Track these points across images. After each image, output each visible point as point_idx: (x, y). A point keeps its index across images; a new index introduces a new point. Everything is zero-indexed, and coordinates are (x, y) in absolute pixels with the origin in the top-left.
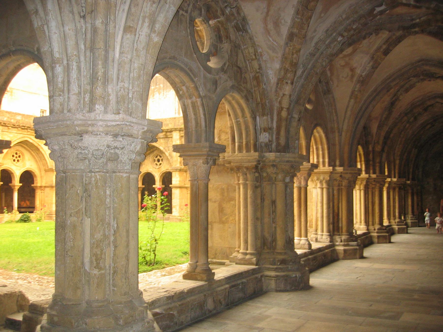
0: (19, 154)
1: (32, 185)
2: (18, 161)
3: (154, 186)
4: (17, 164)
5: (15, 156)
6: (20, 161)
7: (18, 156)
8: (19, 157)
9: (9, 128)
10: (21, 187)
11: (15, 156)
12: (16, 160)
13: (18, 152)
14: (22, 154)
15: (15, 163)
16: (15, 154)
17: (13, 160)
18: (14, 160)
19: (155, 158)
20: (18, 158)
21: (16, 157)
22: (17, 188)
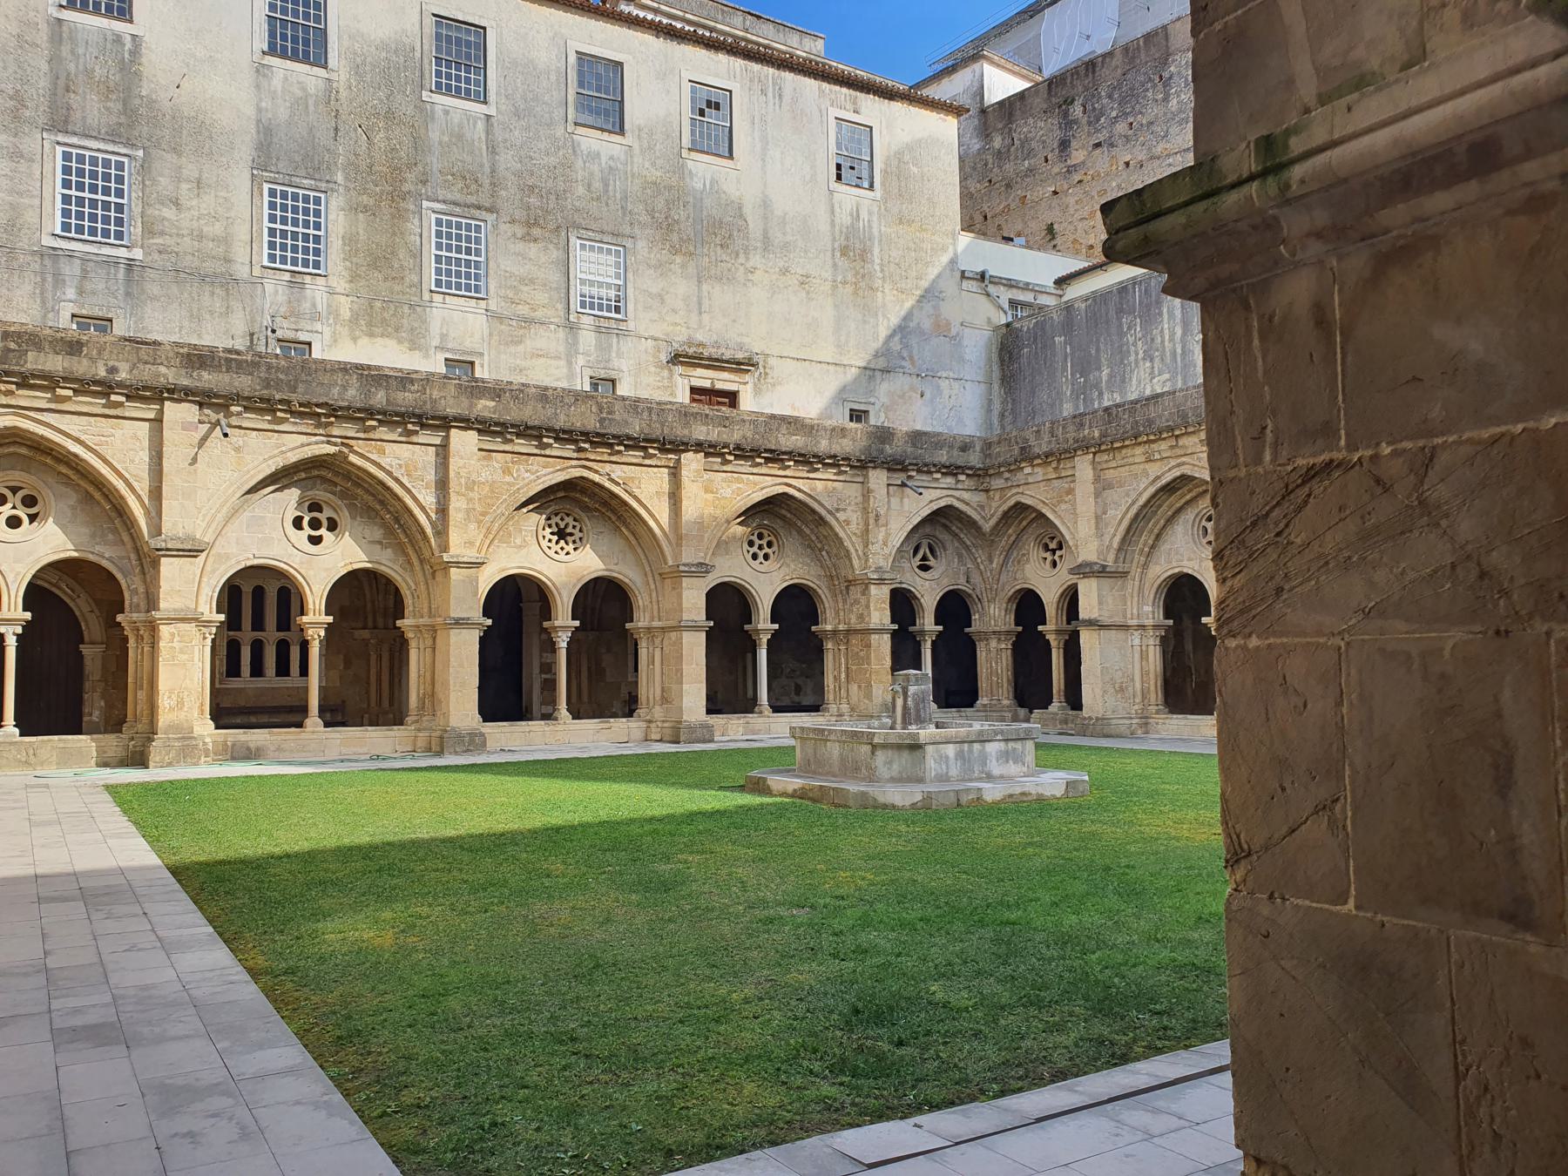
1: (814, 628)
2: (766, 557)
3: (1040, 628)
4: (761, 568)
5: (757, 542)
7: (764, 542)
8: (770, 545)
10: (775, 634)
11: (757, 542)
12: (761, 554)
13: (765, 532)
14: (775, 536)
15: (755, 564)
16: (755, 538)
17: (749, 557)
18: (755, 557)
19: (1204, 523)
20: (767, 550)
21: (760, 547)
22: (765, 638)
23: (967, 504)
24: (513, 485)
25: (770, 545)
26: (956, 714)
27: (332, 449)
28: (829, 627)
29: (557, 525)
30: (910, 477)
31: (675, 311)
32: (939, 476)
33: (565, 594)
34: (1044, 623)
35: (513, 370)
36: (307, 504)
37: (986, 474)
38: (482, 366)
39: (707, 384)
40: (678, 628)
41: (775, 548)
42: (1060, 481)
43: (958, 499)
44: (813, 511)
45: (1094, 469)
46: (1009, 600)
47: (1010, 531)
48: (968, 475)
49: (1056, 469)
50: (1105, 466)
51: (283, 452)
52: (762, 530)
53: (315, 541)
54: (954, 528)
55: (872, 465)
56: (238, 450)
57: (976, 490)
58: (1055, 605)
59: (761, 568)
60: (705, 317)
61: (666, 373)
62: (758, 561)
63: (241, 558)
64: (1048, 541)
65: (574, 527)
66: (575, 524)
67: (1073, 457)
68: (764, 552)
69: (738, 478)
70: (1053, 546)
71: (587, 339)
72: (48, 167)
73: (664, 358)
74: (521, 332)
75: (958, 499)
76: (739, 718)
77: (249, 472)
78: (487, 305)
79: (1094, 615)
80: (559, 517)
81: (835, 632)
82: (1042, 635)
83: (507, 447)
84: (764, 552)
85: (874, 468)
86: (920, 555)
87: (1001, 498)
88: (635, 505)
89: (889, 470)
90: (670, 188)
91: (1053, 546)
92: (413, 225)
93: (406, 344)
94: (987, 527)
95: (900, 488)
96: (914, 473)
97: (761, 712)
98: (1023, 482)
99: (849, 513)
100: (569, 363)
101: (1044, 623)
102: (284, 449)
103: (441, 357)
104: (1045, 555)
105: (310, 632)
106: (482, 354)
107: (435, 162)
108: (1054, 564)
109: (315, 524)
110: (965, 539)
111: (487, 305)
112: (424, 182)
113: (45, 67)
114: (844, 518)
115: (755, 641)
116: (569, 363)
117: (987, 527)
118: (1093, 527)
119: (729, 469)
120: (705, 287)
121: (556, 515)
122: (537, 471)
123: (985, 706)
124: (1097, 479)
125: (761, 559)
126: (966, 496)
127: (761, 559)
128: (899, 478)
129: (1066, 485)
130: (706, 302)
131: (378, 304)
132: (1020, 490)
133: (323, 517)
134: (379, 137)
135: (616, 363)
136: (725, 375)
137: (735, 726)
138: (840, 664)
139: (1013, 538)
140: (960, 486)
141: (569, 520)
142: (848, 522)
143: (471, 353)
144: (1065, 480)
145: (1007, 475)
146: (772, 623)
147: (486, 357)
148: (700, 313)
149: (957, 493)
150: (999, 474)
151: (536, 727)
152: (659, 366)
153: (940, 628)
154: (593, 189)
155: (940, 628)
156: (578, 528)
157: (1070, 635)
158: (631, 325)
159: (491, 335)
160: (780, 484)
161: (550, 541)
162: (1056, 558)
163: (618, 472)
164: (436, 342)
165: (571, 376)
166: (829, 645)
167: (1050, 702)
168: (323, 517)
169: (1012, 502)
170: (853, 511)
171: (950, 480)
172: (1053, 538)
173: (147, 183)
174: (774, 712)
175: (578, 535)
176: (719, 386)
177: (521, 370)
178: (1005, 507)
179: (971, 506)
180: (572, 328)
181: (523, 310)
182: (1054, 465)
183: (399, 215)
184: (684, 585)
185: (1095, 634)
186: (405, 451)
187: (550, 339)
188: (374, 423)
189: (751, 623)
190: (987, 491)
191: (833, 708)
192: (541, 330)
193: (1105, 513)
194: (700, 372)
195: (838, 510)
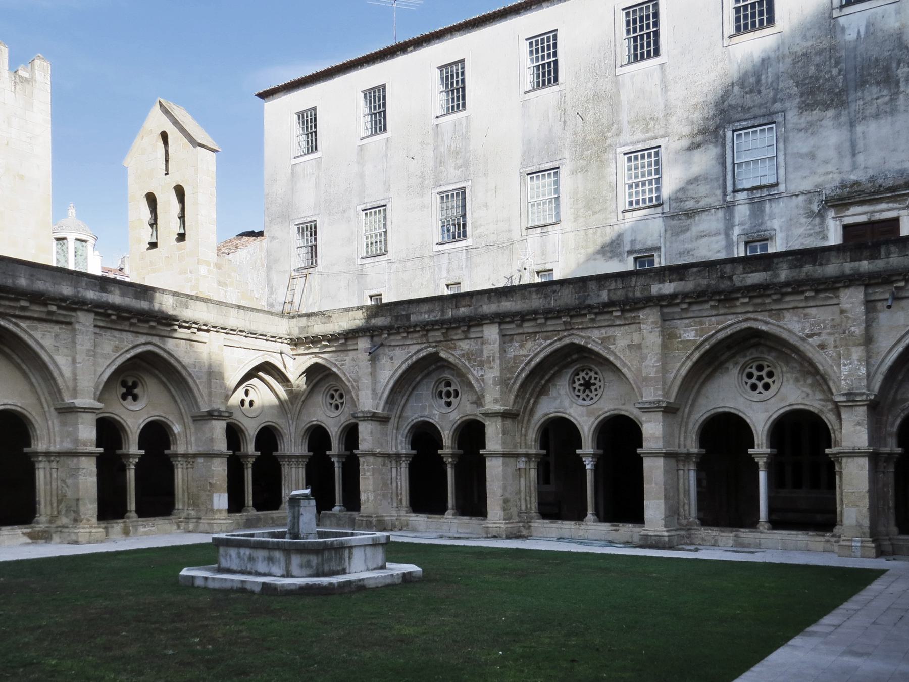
0: (768, 366)
2: (767, 387)
4: (761, 397)
5: (756, 374)
13: (765, 364)
17: (748, 387)
20: (766, 380)
21: (760, 378)
24: (527, 356)
25: (770, 375)
27: (431, 350)
29: (584, 378)
31: (826, 162)
33: (586, 429)
35: (681, 254)
36: (444, 383)
38: (660, 256)
39: (863, 219)
40: (505, 455)
51: (411, 356)
52: (760, 362)
53: (449, 404)
56: (391, 358)
59: (761, 397)
60: (860, 158)
61: (817, 220)
63: (413, 418)
65: (596, 379)
66: (596, 376)
69: (701, 321)
71: (742, 211)
72: (434, 208)
73: (815, 208)
74: (689, 222)
77: (397, 370)
78: (663, 209)
80: (585, 372)
83: (521, 331)
88: (612, 358)
90: (820, 53)
92: (611, 169)
93: (609, 254)
99: (824, 337)
100: (727, 235)
102: (410, 354)
103: (631, 259)
105: (445, 460)
106: (658, 249)
107: (625, 117)
109: (449, 394)
111: (663, 209)
112: (618, 135)
113: (432, 154)
114: (818, 342)
116: (727, 235)
120: (859, 129)
121: (583, 371)
122: (542, 344)
125: (760, 388)
127: (760, 388)
130: (860, 144)
131: (591, 231)
133: (451, 389)
134: (589, 118)
135: (768, 224)
136: (884, 206)
137: (724, 539)
141: (592, 374)
142: (822, 346)
143: (647, 250)
147: (663, 249)
148: (854, 155)
151: (567, 527)
152: (811, 215)
154: (746, 84)
156: (598, 380)
158: (782, 188)
159: (665, 231)
161: (579, 391)
163: (596, 334)
164: (627, 248)
165: (729, 245)
168: (445, 390)
170: (829, 334)
173: (473, 199)
175: (598, 384)
176: (877, 217)
177: (688, 252)
180: (729, 207)
181: (690, 204)
183: (603, 164)
186: (465, 345)
187: (712, 222)
188: (444, 331)
192: (704, 216)
194: (854, 210)
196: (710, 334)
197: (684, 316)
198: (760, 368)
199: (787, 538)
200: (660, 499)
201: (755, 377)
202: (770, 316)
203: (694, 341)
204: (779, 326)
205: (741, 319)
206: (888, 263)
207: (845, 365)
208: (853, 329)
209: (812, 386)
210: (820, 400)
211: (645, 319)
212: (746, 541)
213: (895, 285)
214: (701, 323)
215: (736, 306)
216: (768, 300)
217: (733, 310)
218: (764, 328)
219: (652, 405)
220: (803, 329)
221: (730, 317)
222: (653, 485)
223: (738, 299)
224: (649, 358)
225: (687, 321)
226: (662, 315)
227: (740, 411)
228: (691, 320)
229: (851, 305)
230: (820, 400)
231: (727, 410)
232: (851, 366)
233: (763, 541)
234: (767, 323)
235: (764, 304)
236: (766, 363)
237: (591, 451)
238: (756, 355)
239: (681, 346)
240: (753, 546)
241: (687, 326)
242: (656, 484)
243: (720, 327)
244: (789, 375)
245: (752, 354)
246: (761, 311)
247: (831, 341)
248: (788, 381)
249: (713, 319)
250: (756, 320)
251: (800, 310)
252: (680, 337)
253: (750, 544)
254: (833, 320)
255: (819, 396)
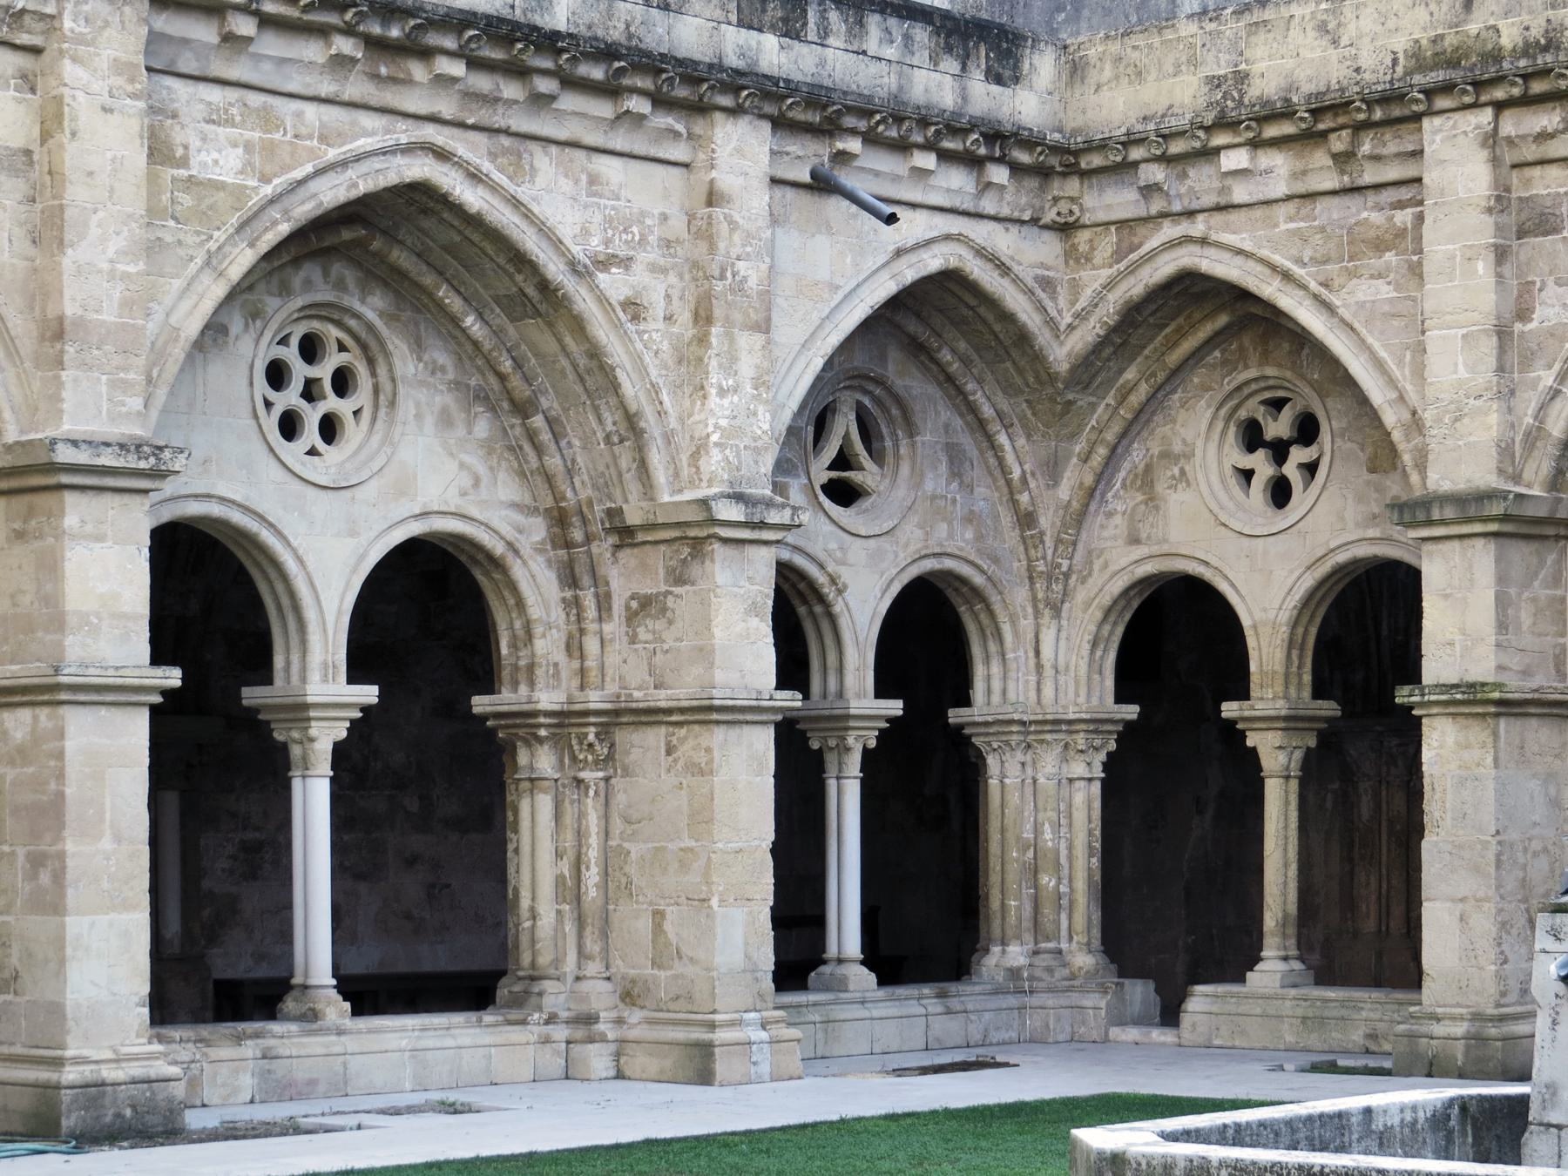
0: (342, 348)
1: (481, 704)
4: (315, 470)
5: (300, 371)
6: (353, 433)
7: (323, 372)
9: (228, 38)
10: (365, 725)
11: (300, 371)
14: (364, 347)
15: (292, 452)
16: (291, 354)
17: (271, 423)
18: (289, 426)
20: (331, 403)
21: (310, 392)
22: (326, 735)
23: (1004, 269)
25: (342, 382)
26: (935, 1006)
28: (548, 699)
30: (842, 157)
32: (927, 160)
34: (1243, 694)
37: (1072, 170)
41: (361, 396)
42: (1353, 202)
43: (980, 252)
44: (521, 260)
45: (1495, 161)
46: (1108, 612)
47: (1130, 374)
48: (1016, 169)
49: (1343, 160)
50: (1530, 152)
52: (316, 325)
54: (946, 356)
55: (726, 101)
57: (1034, 221)
58: (1284, 631)
62: (301, 445)
64: (1260, 414)
67: (1417, 118)
68: (322, 408)
69: (266, 108)
70: (1278, 427)
75: (980, 252)
76: (239, 1039)
79: (1482, 668)
81: (566, 719)
82: (1232, 734)
84: (322, 408)
85: (735, 112)
86: (830, 452)
87: (1118, 256)
89: (781, 124)
91: (1278, 427)
94: (1061, 353)
95: (805, 199)
96: (854, 145)
97: (311, 1016)
98: (1209, 200)
101: (1243, 694)
104: (1248, 461)
108: (1280, 493)
110: (979, 397)
115: (284, 748)
117: (1061, 353)
118: (1492, 362)
119: (233, 73)
123: (1014, 973)
124: (1501, 201)
126: (1003, 241)
128: (804, 157)
129: (1376, 217)
132: (1198, 227)
137: (224, 1069)
138: (580, 835)
139: (1135, 399)
140: (989, 205)
142: (634, 308)
144: (1372, 198)
145: (1155, 173)
146: (351, 680)
149: (980, 232)
150: (1127, 167)
153: (895, 707)
155: (895, 707)
157: (1322, 735)
160: (409, 149)
162: (1290, 470)
166: (544, 761)
167: (1252, 958)
169: (1164, 268)
170: (654, 268)
171: (955, 182)
172: (1277, 405)
174: (357, 1012)
178: (1136, 287)
179: (1017, 280)
182: (1339, 143)
184: (71, 521)
185: (1478, 733)
189: (268, 681)
190: (1065, 229)
191: (554, 996)
193: (1523, 314)
195: (604, 263)
196: (298, 174)
197: (219, 69)
198: (311, 349)
199: (430, 1043)
200: (127, 906)
201: (296, 385)
202: (493, 156)
203: (239, 193)
204: (516, 203)
205: (404, 139)
206: (822, 63)
207: (722, 392)
208: (741, 265)
209: (488, 447)
210: (516, 506)
211: (80, 40)
212: (301, 1070)
213: (840, 145)
214: (268, 121)
215: (408, 82)
216: (511, 90)
217: (391, 97)
218: (471, 197)
219: (131, 462)
220: (586, 232)
221: (368, 120)
222: (106, 844)
223: (427, 54)
224: (94, 232)
225: (215, 94)
226: (155, 39)
227: (262, 518)
228: (233, 94)
229: (741, 180)
230: (516, 506)
231: (215, 510)
232: (736, 399)
233: (355, 1063)
234: (475, 177)
235: (492, 100)
236: (334, 332)
237: (1280, 707)
238: (324, 295)
239: (186, 200)
240: (321, 1088)
241: (217, 118)
242: (118, 839)
243: (332, 154)
244: (422, 395)
245: (308, 285)
246: (474, 127)
247: (656, 293)
248: (419, 417)
249: (310, 110)
250: (442, 155)
251: (580, 155)
252: (184, 162)
253: (312, 1083)
254: (664, 218)
255: (508, 489)
